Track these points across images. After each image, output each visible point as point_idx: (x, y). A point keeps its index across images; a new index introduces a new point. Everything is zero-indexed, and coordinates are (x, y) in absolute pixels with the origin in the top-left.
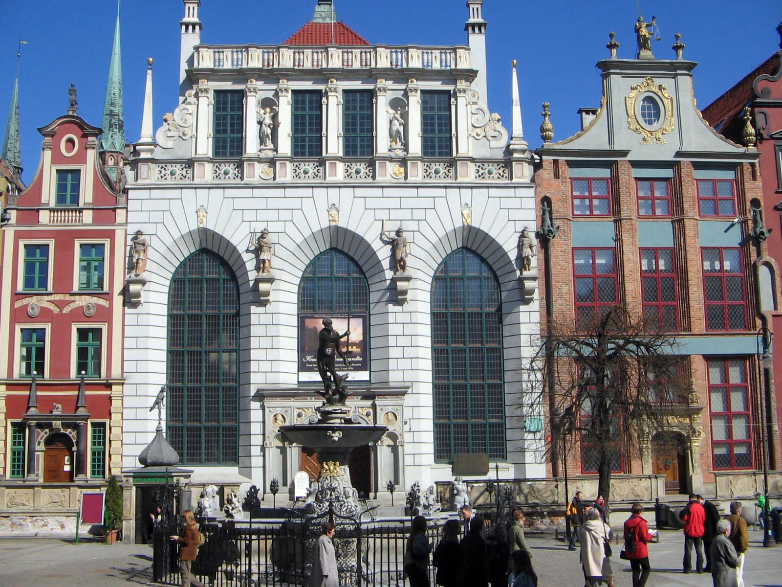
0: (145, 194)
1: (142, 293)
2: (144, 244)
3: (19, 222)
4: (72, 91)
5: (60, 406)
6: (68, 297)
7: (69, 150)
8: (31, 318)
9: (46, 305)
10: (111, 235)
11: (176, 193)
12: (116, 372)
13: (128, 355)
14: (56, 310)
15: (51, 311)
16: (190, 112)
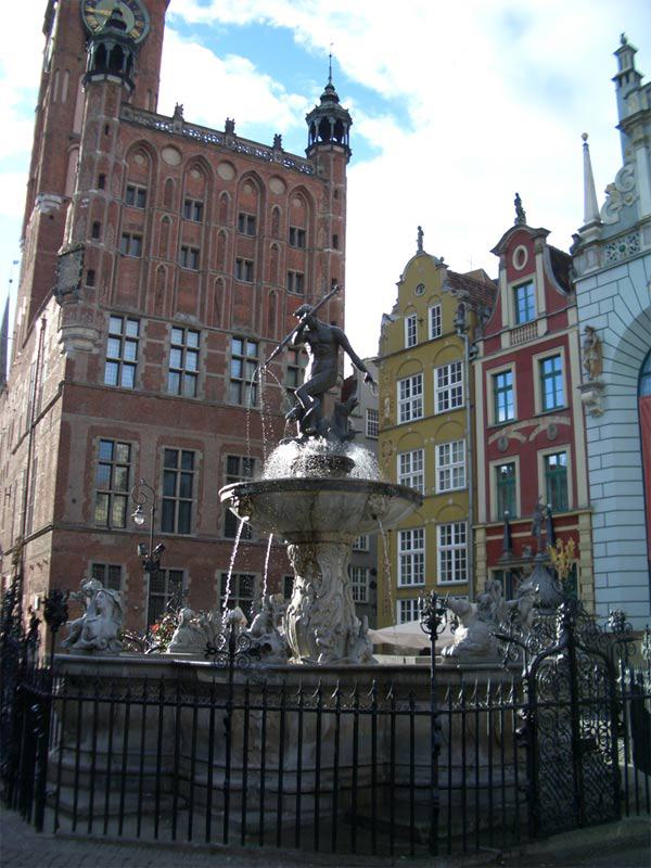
0: (591, 283)
1: (598, 401)
2: (592, 341)
3: (487, 353)
4: (518, 202)
5: (529, 548)
6: (532, 423)
7: (520, 264)
8: (503, 454)
9: (514, 435)
10: (564, 341)
11: (622, 271)
12: (582, 501)
13: (593, 478)
14: (522, 439)
15: (519, 441)
16: (631, 172)
